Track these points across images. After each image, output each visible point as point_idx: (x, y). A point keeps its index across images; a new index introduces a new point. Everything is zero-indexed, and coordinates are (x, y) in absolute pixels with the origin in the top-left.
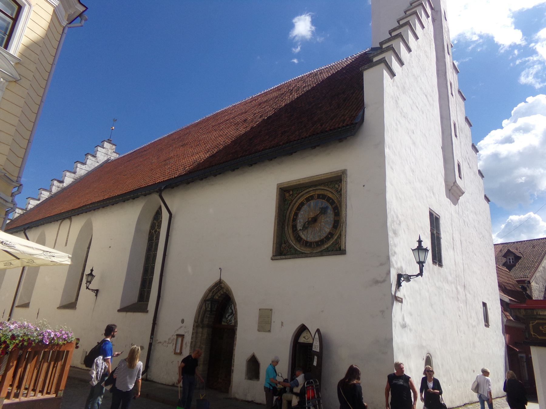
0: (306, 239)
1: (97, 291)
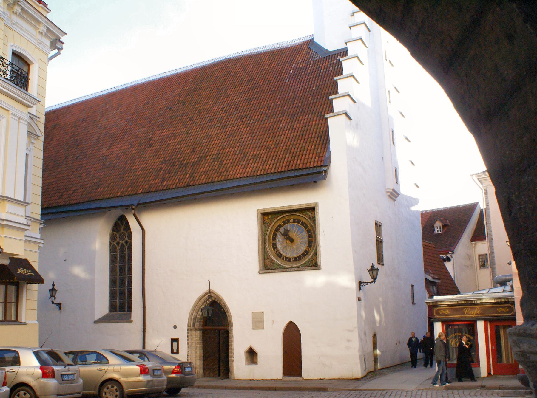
0: (285, 255)
1: (59, 305)
